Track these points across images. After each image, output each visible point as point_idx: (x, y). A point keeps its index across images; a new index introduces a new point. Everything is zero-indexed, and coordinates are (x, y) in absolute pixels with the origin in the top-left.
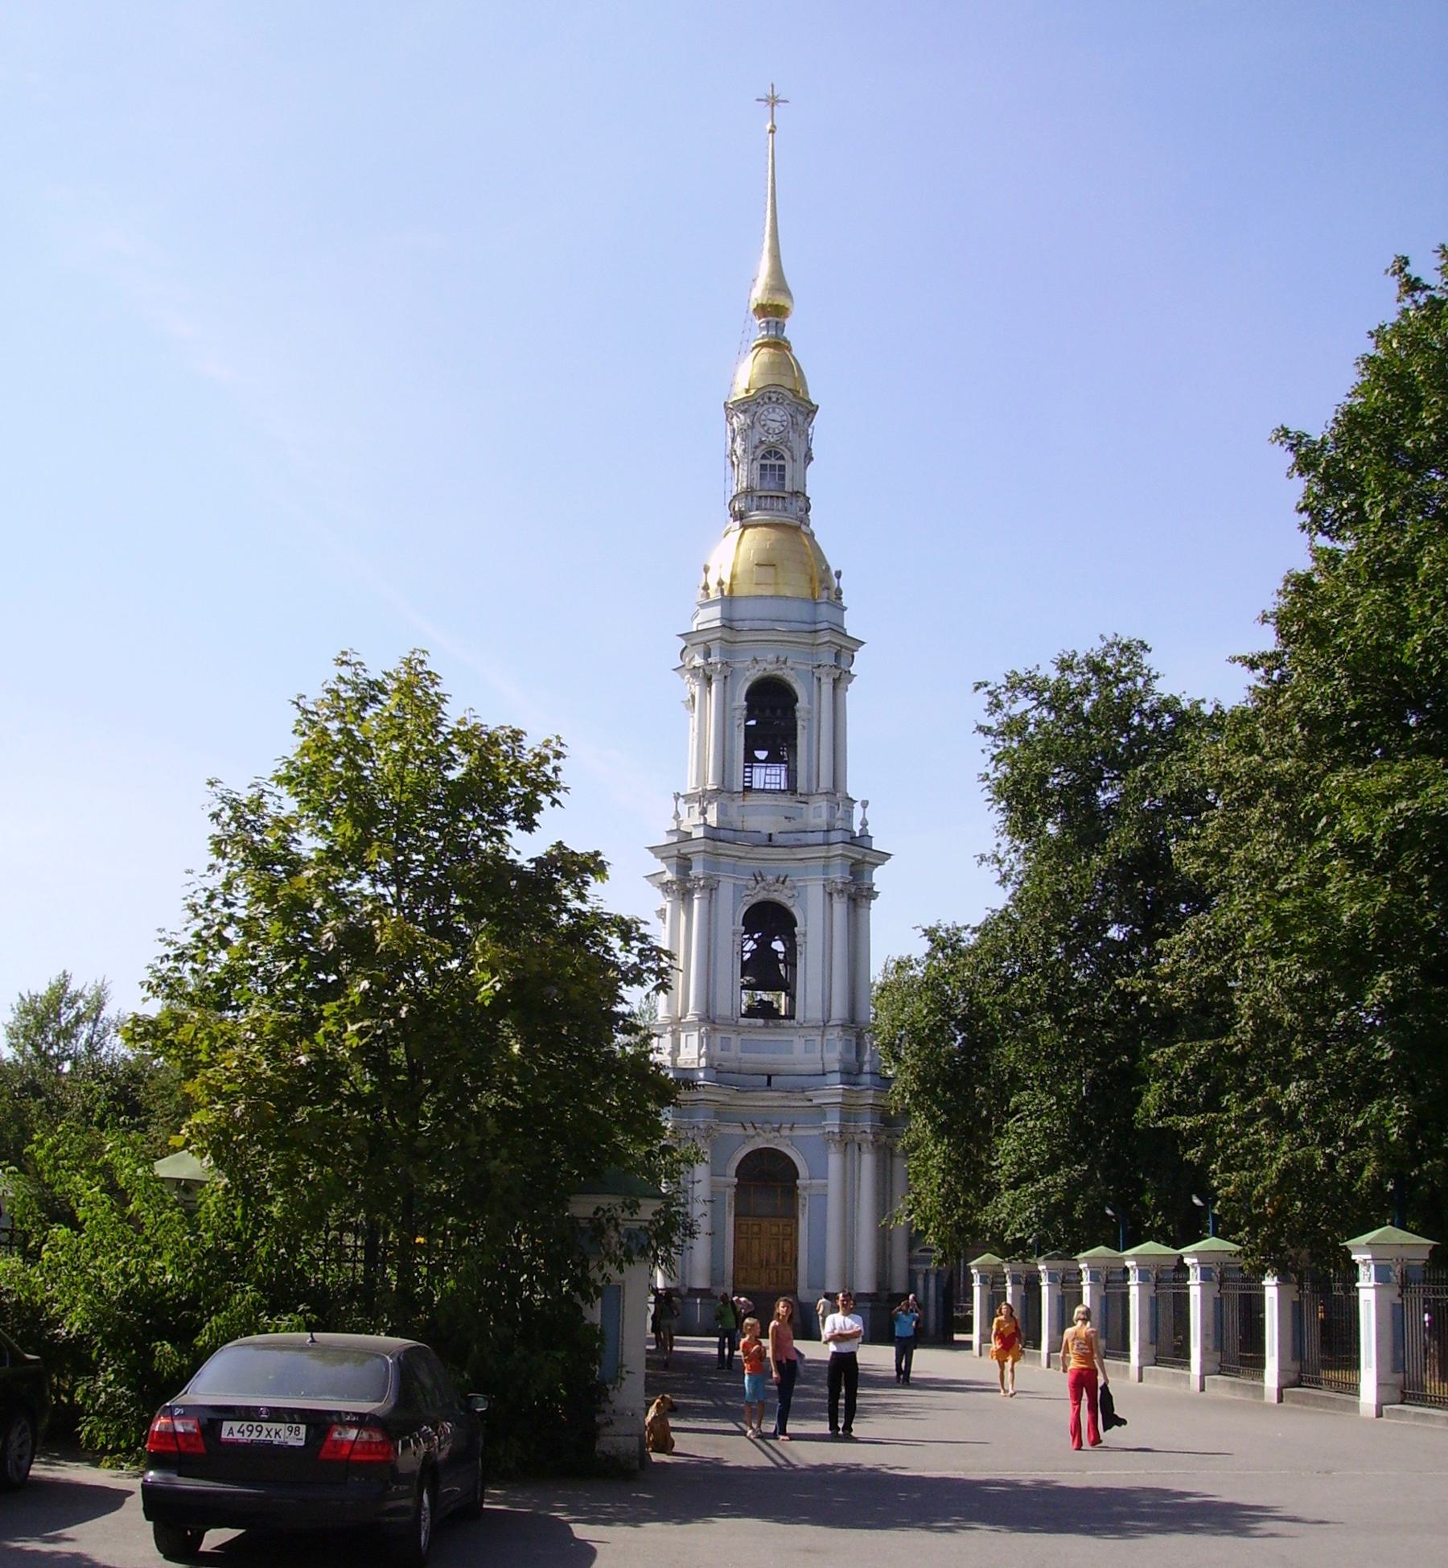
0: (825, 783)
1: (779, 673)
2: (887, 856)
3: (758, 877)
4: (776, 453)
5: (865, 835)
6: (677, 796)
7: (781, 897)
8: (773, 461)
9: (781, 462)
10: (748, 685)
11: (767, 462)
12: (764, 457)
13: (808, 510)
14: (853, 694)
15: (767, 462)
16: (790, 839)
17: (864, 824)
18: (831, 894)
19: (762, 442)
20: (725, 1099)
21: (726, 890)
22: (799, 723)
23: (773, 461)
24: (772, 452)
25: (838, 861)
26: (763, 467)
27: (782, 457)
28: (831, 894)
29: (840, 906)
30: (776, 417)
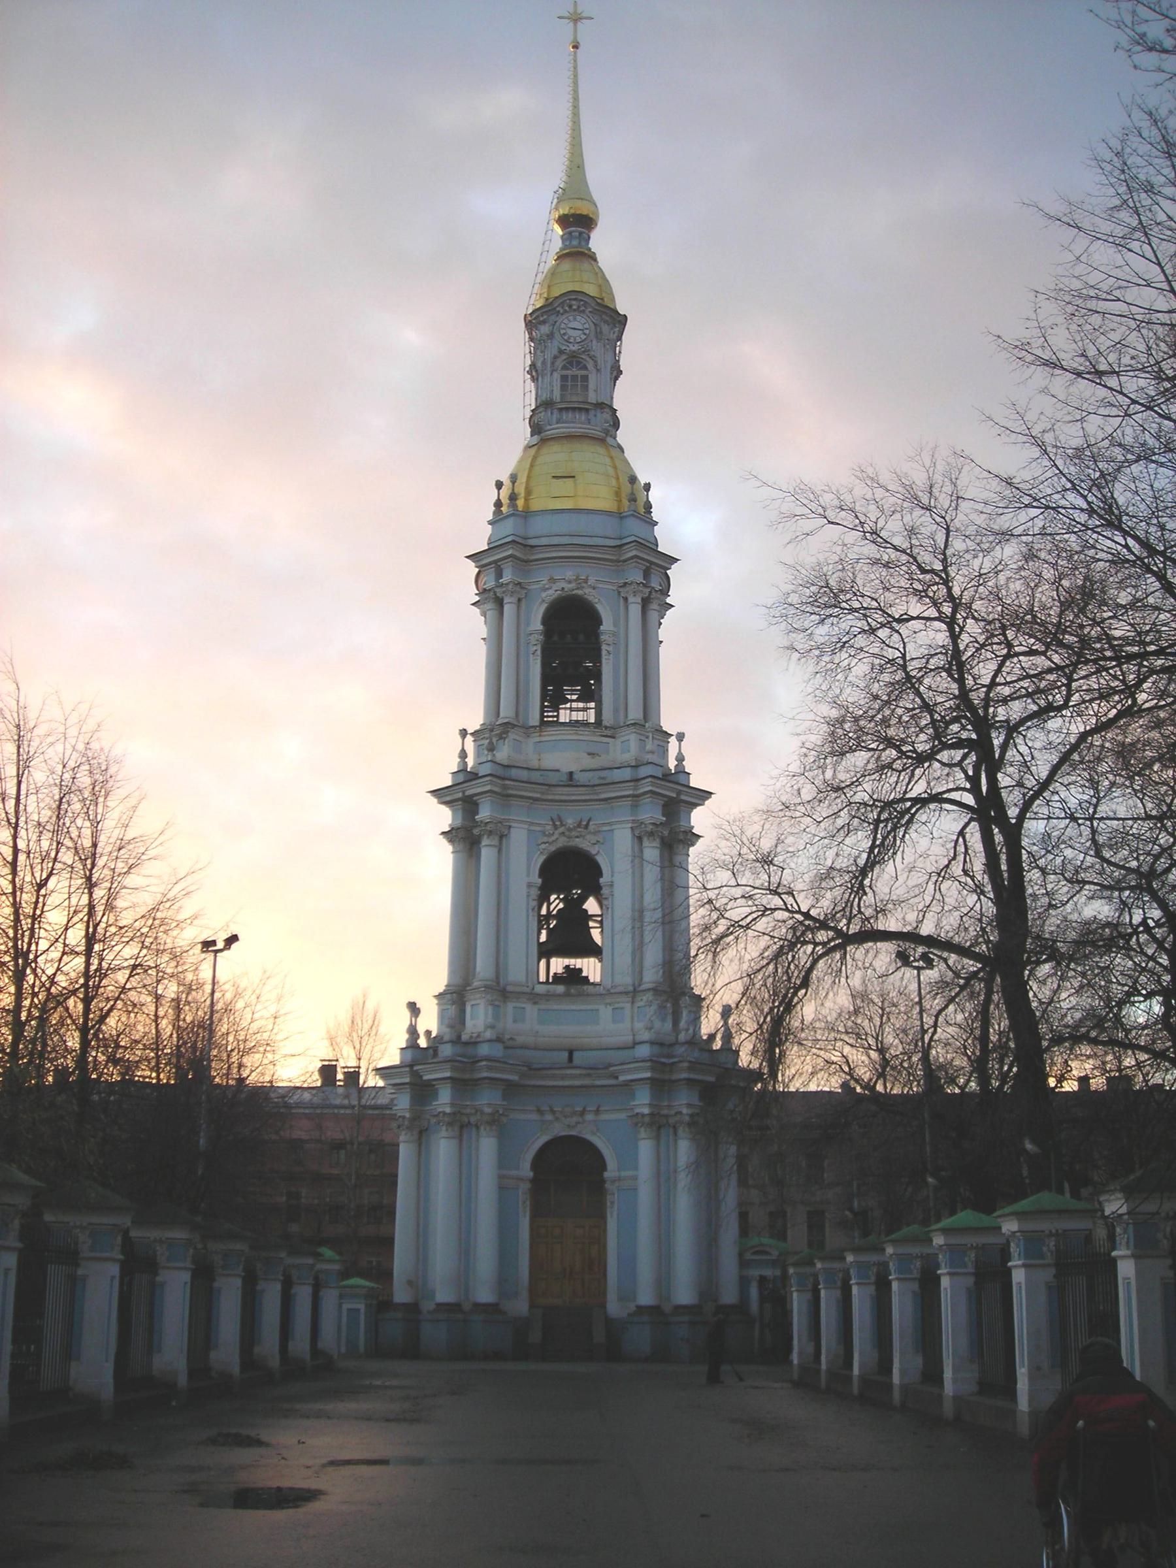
0: (635, 714)
1: (580, 592)
2: (706, 795)
3: (558, 822)
4: (578, 363)
5: (681, 771)
6: (464, 733)
7: (584, 844)
9: (583, 372)
10: (544, 606)
11: (569, 372)
12: (564, 368)
13: (616, 424)
14: (669, 628)
15: (569, 372)
16: (593, 778)
18: (640, 839)
19: (561, 352)
21: (519, 837)
22: (604, 647)
24: (574, 360)
25: (647, 800)
26: (564, 378)
27: (585, 368)
28: (640, 839)
29: (652, 852)
30: (576, 326)
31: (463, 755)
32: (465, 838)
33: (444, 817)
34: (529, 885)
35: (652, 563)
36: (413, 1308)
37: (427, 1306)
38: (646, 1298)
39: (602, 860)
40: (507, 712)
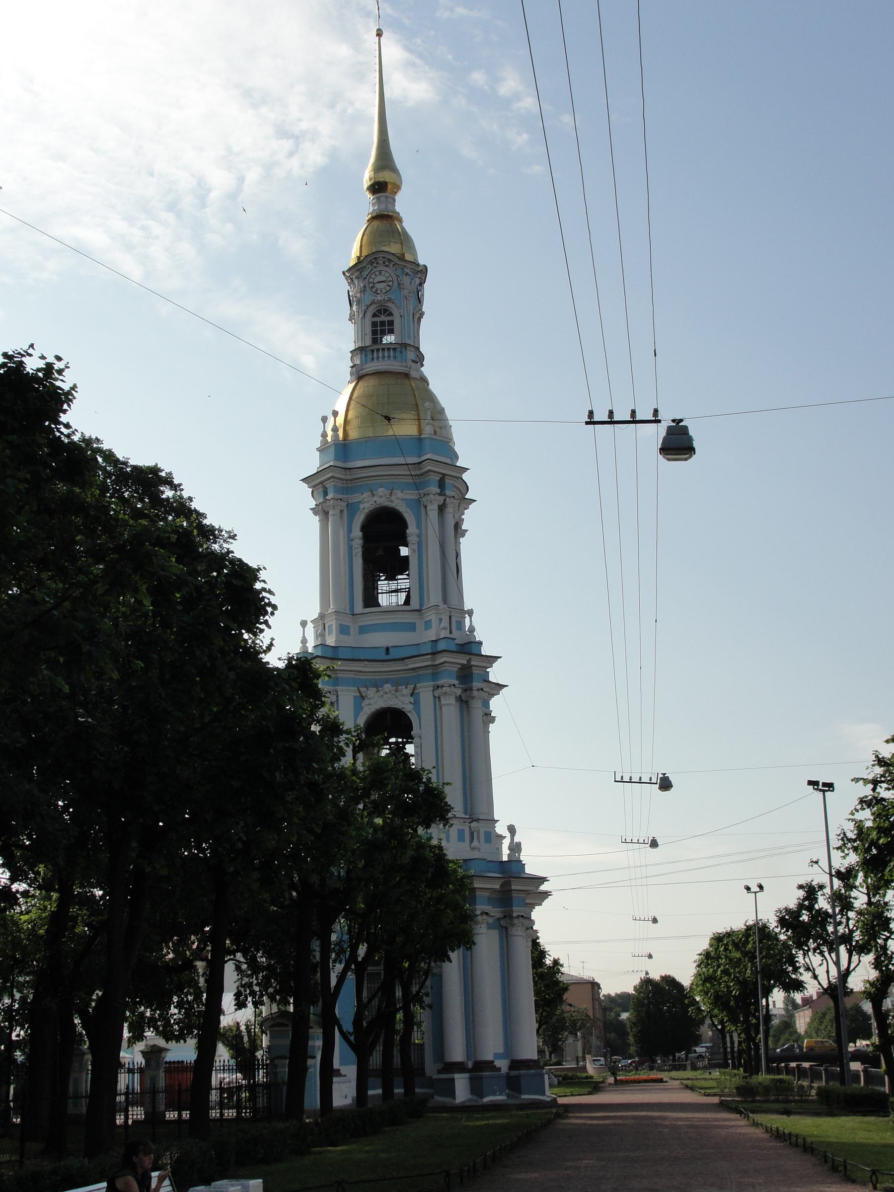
4: (386, 310)
6: (304, 624)
8: (383, 318)
9: (390, 318)
11: (376, 319)
12: (374, 315)
23: (383, 318)
26: (374, 324)
27: (391, 314)
31: (304, 641)
35: (444, 475)
39: (413, 717)
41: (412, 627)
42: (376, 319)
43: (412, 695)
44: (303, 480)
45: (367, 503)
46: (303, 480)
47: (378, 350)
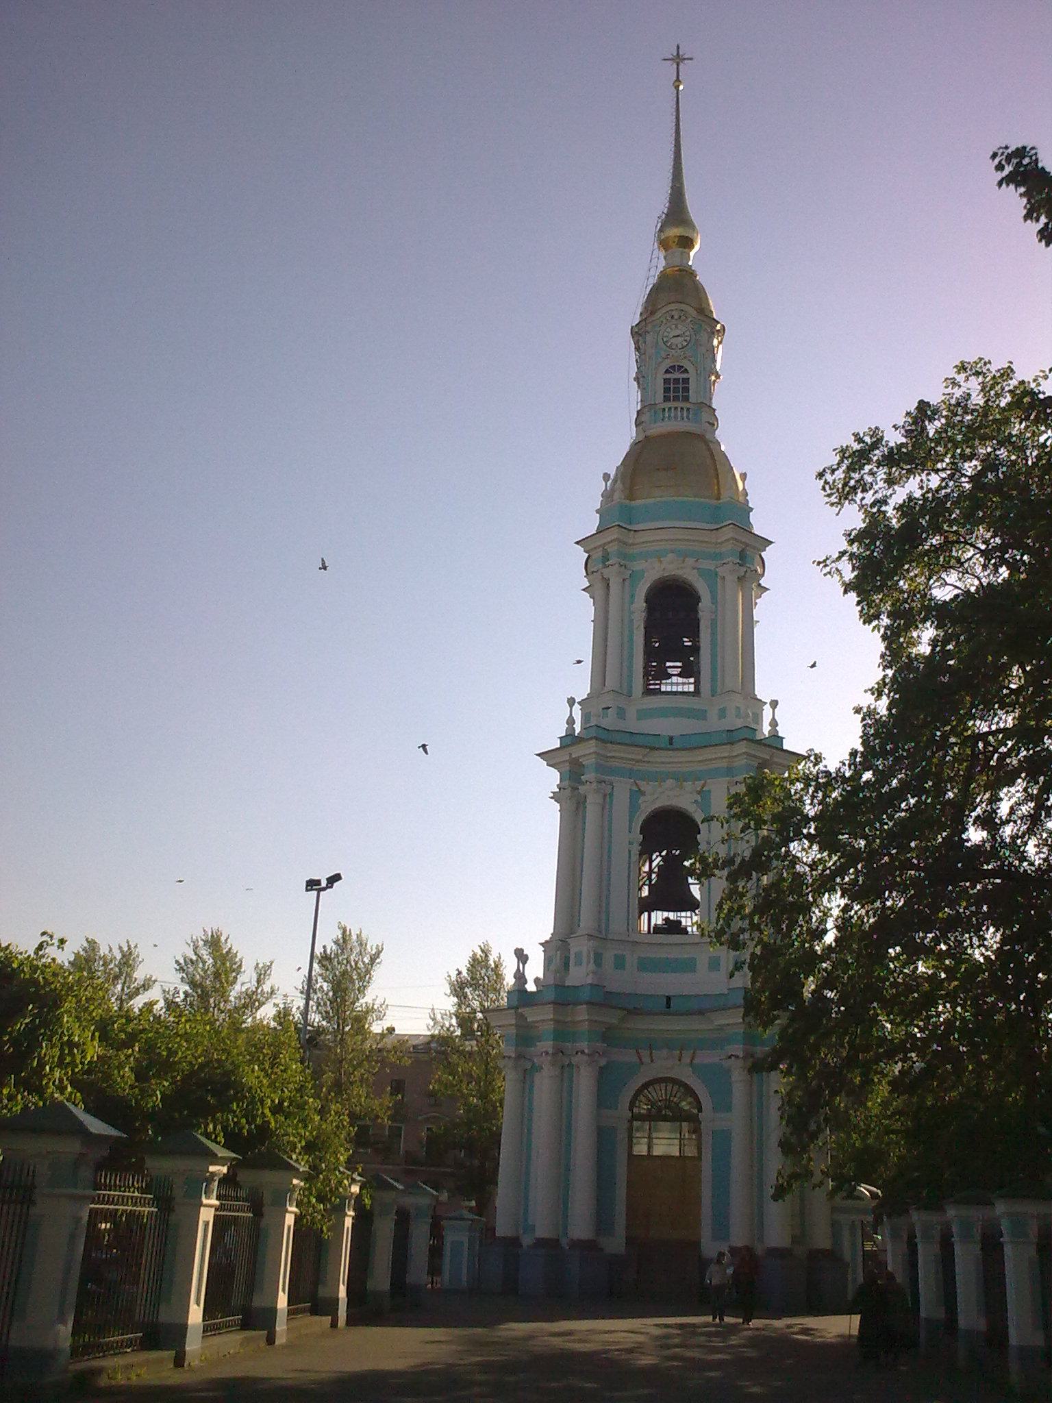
1: (680, 572)
6: (571, 702)
8: (677, 375)
9: (685, 376)
11: (668, 376)
12: (667, 372)
17: (774, 723)
20: (615, 1021)
23: (677, 375)
26: (666, 381)
27: (686, 371)
31: (571, 721)
32: (571, 796)
33: (552, 778)
34: (630, 843)
35: (747, 545)
36: (514, 1242)
37: (527, 1241)
38: (739, 1237)
40: (611, 682)
41: (701, 715)
42: (668, 376)
43: (699, 793)
44: (577, 543)
45: (652, 572)
46: (577, 543)
47: (670, 409)
